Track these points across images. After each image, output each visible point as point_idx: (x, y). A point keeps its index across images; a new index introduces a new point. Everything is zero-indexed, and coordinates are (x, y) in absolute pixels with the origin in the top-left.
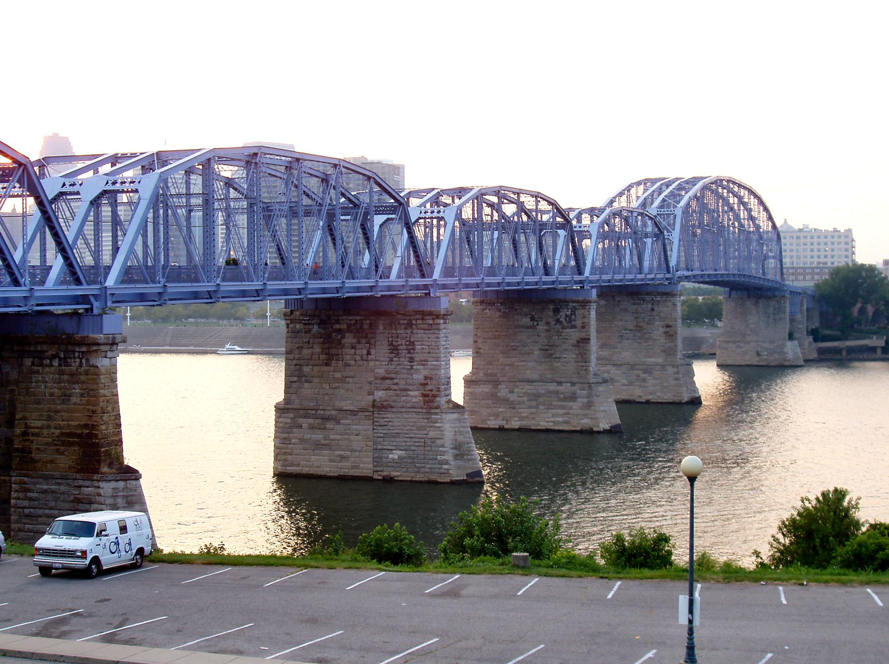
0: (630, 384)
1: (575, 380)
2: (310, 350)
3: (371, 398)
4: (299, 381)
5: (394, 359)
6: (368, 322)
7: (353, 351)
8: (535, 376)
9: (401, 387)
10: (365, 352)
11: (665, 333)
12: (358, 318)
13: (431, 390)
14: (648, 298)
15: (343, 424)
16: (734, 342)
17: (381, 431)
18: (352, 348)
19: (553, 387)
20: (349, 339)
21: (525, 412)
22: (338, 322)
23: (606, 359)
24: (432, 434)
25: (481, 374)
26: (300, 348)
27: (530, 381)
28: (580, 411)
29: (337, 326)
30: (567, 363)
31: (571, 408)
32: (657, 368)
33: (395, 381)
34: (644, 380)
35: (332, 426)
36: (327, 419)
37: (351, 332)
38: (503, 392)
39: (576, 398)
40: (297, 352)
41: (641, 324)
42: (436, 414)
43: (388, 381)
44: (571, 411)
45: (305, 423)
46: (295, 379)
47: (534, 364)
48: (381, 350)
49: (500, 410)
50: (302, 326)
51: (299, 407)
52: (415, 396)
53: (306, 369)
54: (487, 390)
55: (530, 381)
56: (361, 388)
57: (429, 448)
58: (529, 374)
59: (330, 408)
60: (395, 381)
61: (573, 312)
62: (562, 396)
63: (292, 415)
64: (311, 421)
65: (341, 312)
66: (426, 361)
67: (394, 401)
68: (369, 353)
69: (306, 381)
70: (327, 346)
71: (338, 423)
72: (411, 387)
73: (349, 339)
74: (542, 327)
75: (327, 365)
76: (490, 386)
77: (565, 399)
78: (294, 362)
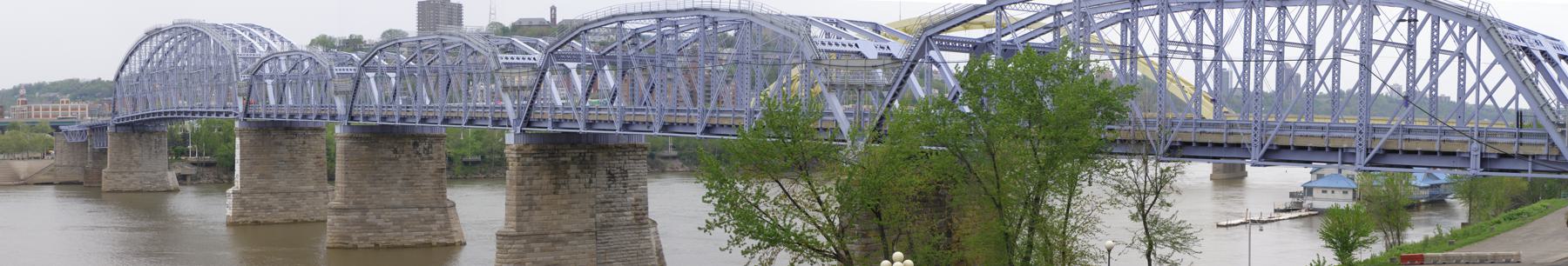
0: (287, 209)
1: (433, 205)
2: (540, 181)
3: (593, 220)
4: (530, 209)
5: (613, 185)
6: (590, 154)
7: (577, 180)
8: (399, 203)
9: (618, 208)
10: (588, 180)
11: (315, 163)
12: (583, 151)
13: (641, 210)
14: (300, 133)
15: (571, 245)
16: (120, 173)
17: (603, 247)
18: (577, 177)
19: (415, 212)
20: (573, 170)
21: (391, 235)
22: (564, 155)
23: (265, 189)
24: (643, 246)
25: (351, 203)
26: (531, 180)
27: (395, 208)
28: (438, 233)
29: (563, 159)
30: (426, 189)
31: (431, 230)
32: (310, 194)
33: (613, 204)
34: (299, 206)
35: (561, 248)
36: (559, 241)
37: (575, 163)
38: (371, 217)
39: (435, 221)
40: (527, 183)
41: (295, 156)
42: (645, 228)
43: (608, 205)
44: (432, 233)
45: (537, 247)
46: (526, 208)
47: (398, 192)
48: (601, 178)
49: (369, 234)
50: (532, 159)
51: (532, 233)
52: (629, 216)
53: (536, 198)
54: (357, 217)
55: (395, 208)
56: (584, 212)
57: (640, 258)
58: (393, 201)
59: (559, 231)
60: (613, 204)
61: (430, 147)
62: (422, 220)
63: (525, 241)
64: (541, 245)
65: (569, 146)
66: (637, 186)
67: (613, 221)
68: (591, 182)
69: (536, 209)
70: (554, 176)
71: (567, 244)
72: (625, 208)
73: (573, 170)
74: (403, 159)
75: (554, 193)
76: (359, 213)
77: (426, 222)
78: (525, 193)
